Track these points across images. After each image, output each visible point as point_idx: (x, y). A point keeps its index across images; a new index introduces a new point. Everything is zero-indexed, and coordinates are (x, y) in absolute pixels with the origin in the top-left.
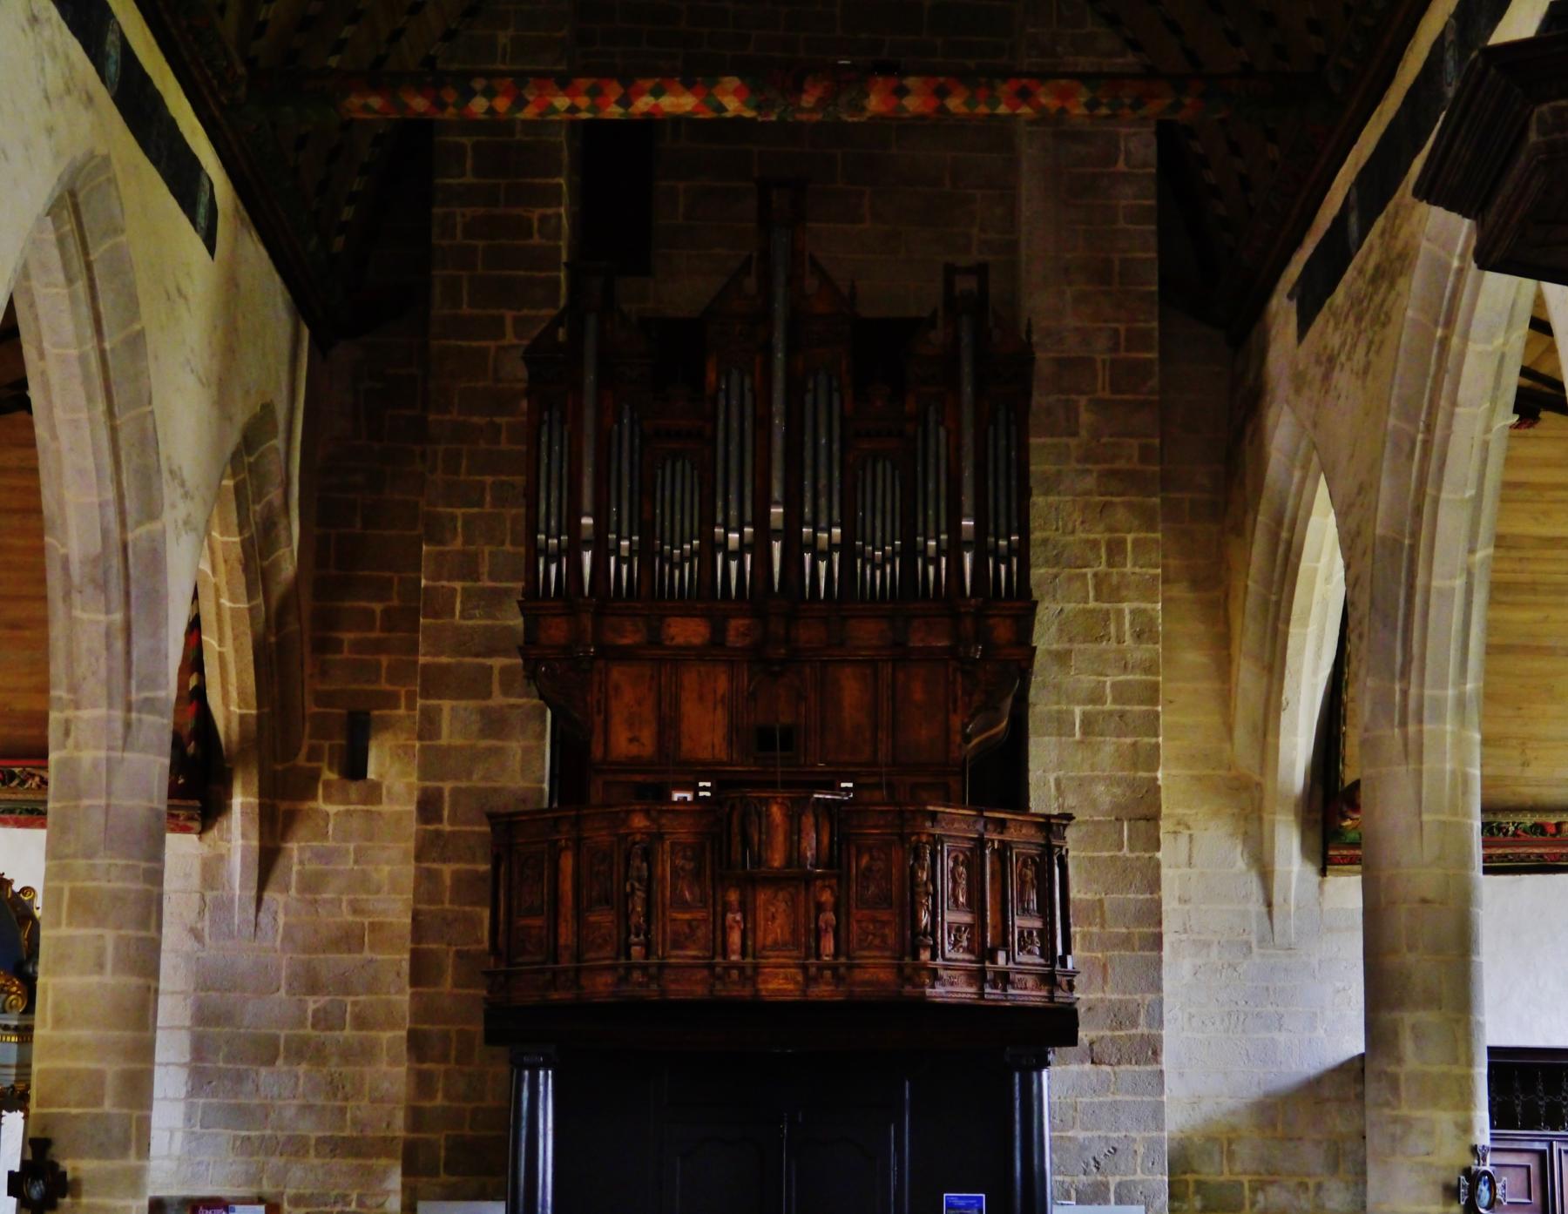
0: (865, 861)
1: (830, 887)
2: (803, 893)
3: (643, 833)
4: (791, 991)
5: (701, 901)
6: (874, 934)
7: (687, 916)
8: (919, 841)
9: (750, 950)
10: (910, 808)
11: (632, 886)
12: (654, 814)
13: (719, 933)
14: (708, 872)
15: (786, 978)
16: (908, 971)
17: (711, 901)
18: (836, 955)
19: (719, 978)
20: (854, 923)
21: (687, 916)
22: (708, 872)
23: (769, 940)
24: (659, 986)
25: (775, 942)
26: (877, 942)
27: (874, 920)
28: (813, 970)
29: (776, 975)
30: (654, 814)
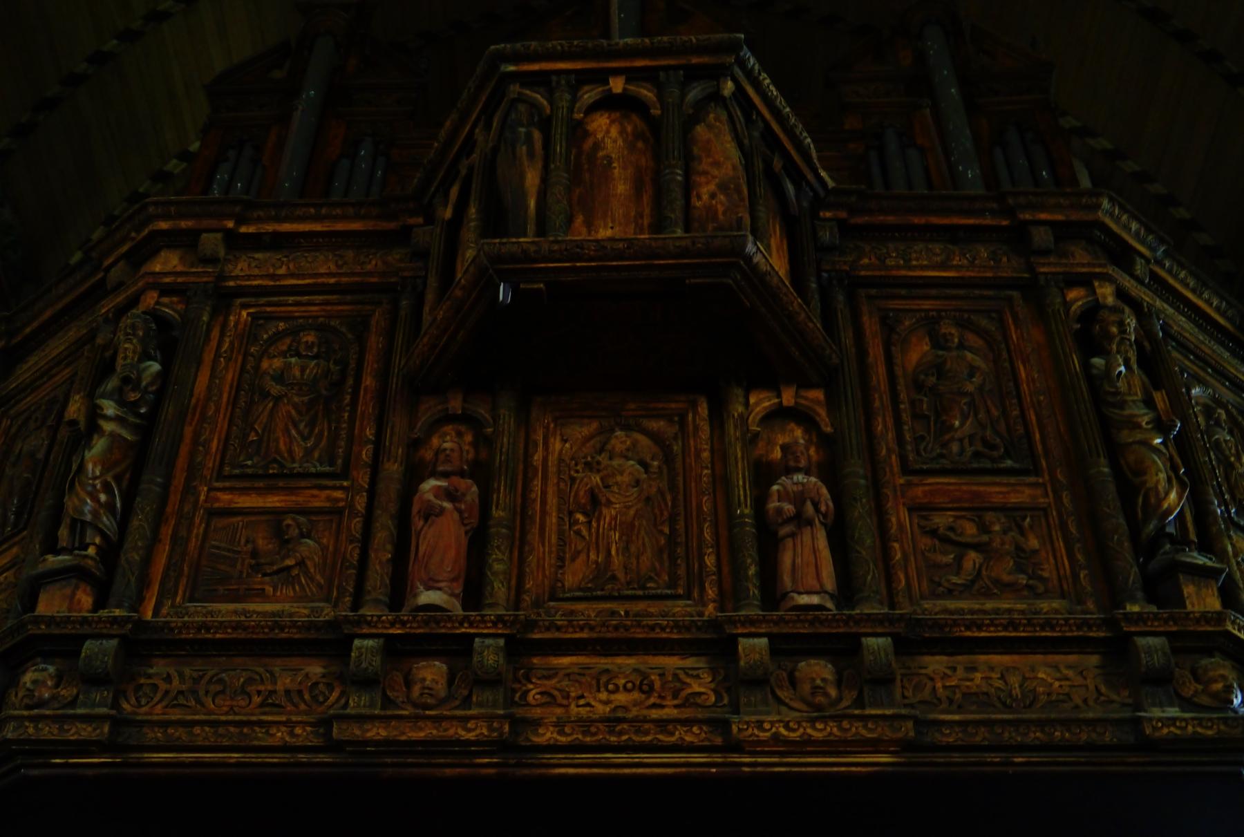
0: (918, 351)
1: (801, 416)
2: (705, 428)
3: (166, 291)
4: (662, 724)
5: (332, 463)
6: (977, 547)
7: (273, 501)
8: (1093, 311)
9: (499, 590)
10: (1043, 216)
11: (94, 414)
12: (211, 242)
13: (383, 534)
14: (368, 381)
15: (646, 688)
16: (1152, 646)
17: (366, 454)
18: (847, 591)
19: (366, 682)
20: (904, 514)
21: (273, 501)
22: (368, 381)
23: (574, 575)
24: (115, 705)
25: (602, 573)
26: (1004, 570)
27: (978, 510)
28: (754, 648)
29: (603, 680)
30: (211, 242)
